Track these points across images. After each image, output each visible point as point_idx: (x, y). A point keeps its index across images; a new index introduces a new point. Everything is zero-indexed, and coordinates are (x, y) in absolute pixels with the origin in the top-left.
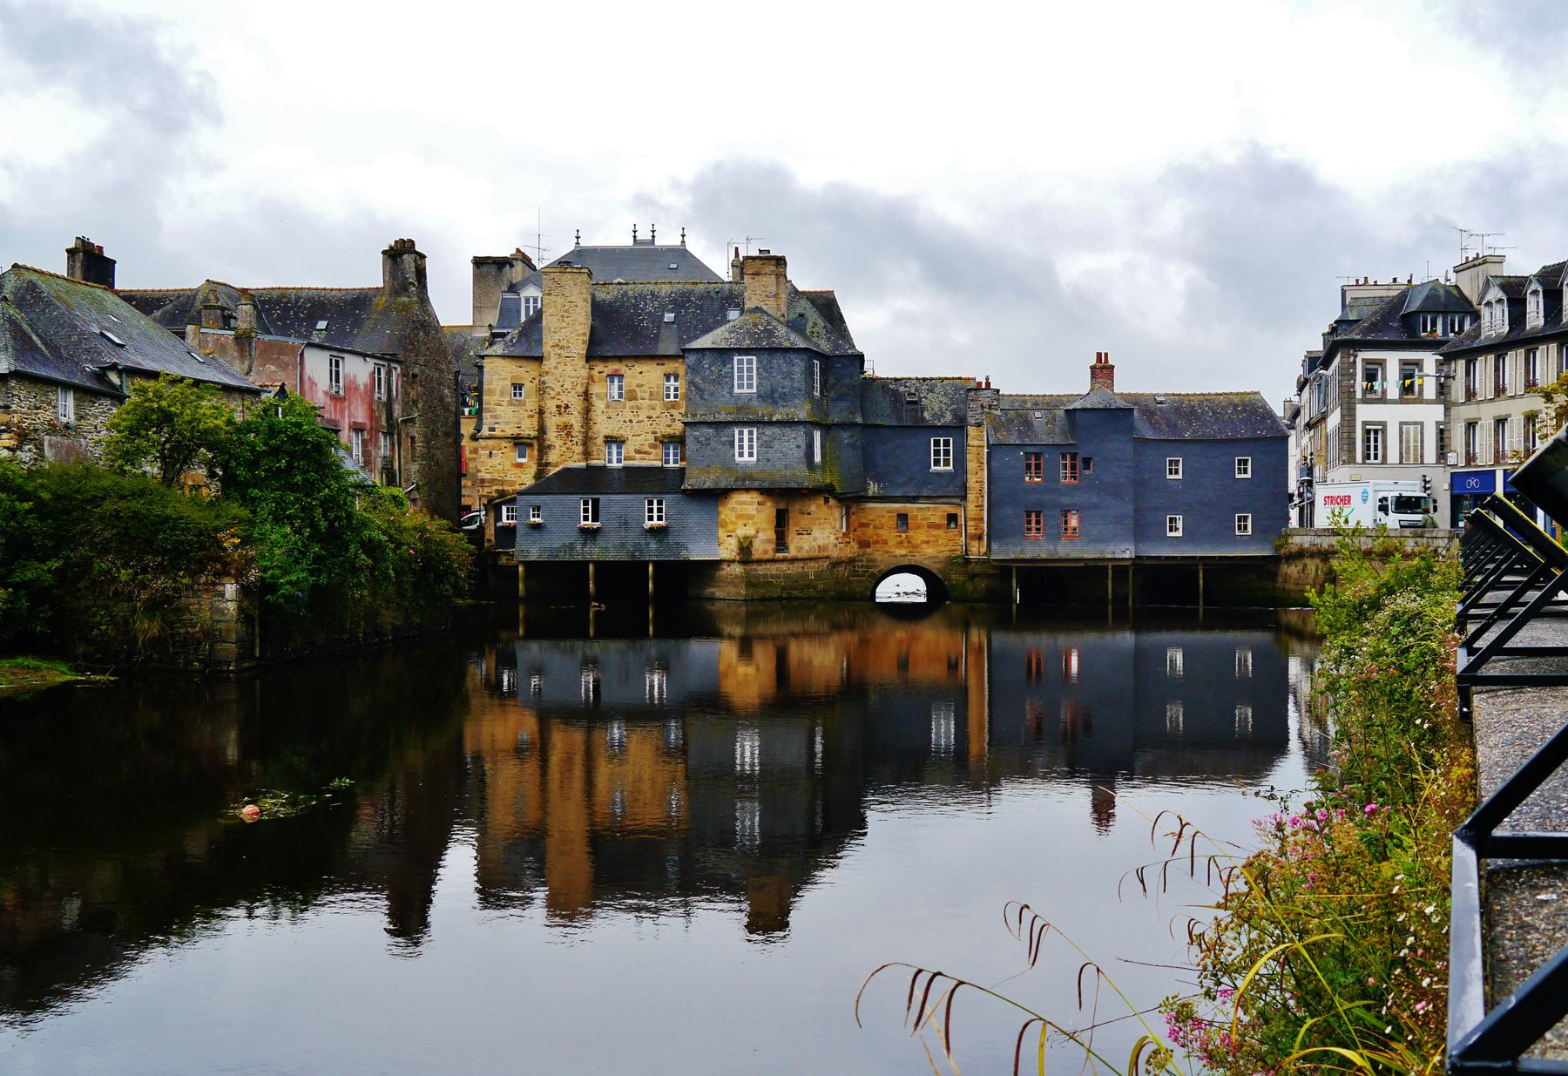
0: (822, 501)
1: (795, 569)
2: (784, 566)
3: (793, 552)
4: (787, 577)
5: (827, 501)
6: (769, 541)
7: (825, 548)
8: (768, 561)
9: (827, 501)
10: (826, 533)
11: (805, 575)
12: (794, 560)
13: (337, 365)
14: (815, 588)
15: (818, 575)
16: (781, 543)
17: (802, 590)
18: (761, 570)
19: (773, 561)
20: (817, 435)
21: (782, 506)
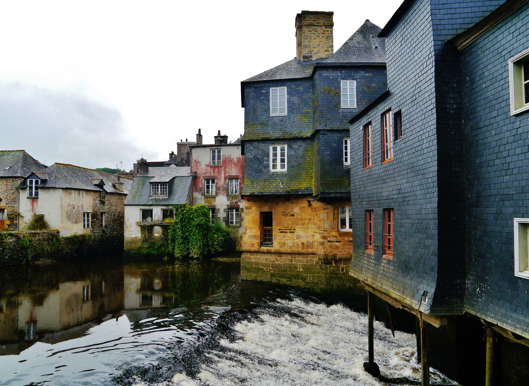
0: (305, 204)
1: (283, 261)
2: (272, 258)
3: (276, 246)
4: (275, 267)
5: (310, 205)
6: (254, 237)
7: (309, 245)
8: (255, 252)
9: (310, 205)
10: (311, 232)
11: (294, 268)
12: (279, 253)
13: (219, 152)
14: (304, 279)
15: (307, 269)
16: (266, 237)
17: (290, 278)
18: (253, 258)
19: (258, 252)
20: (286, 147)
21: (266, 209)
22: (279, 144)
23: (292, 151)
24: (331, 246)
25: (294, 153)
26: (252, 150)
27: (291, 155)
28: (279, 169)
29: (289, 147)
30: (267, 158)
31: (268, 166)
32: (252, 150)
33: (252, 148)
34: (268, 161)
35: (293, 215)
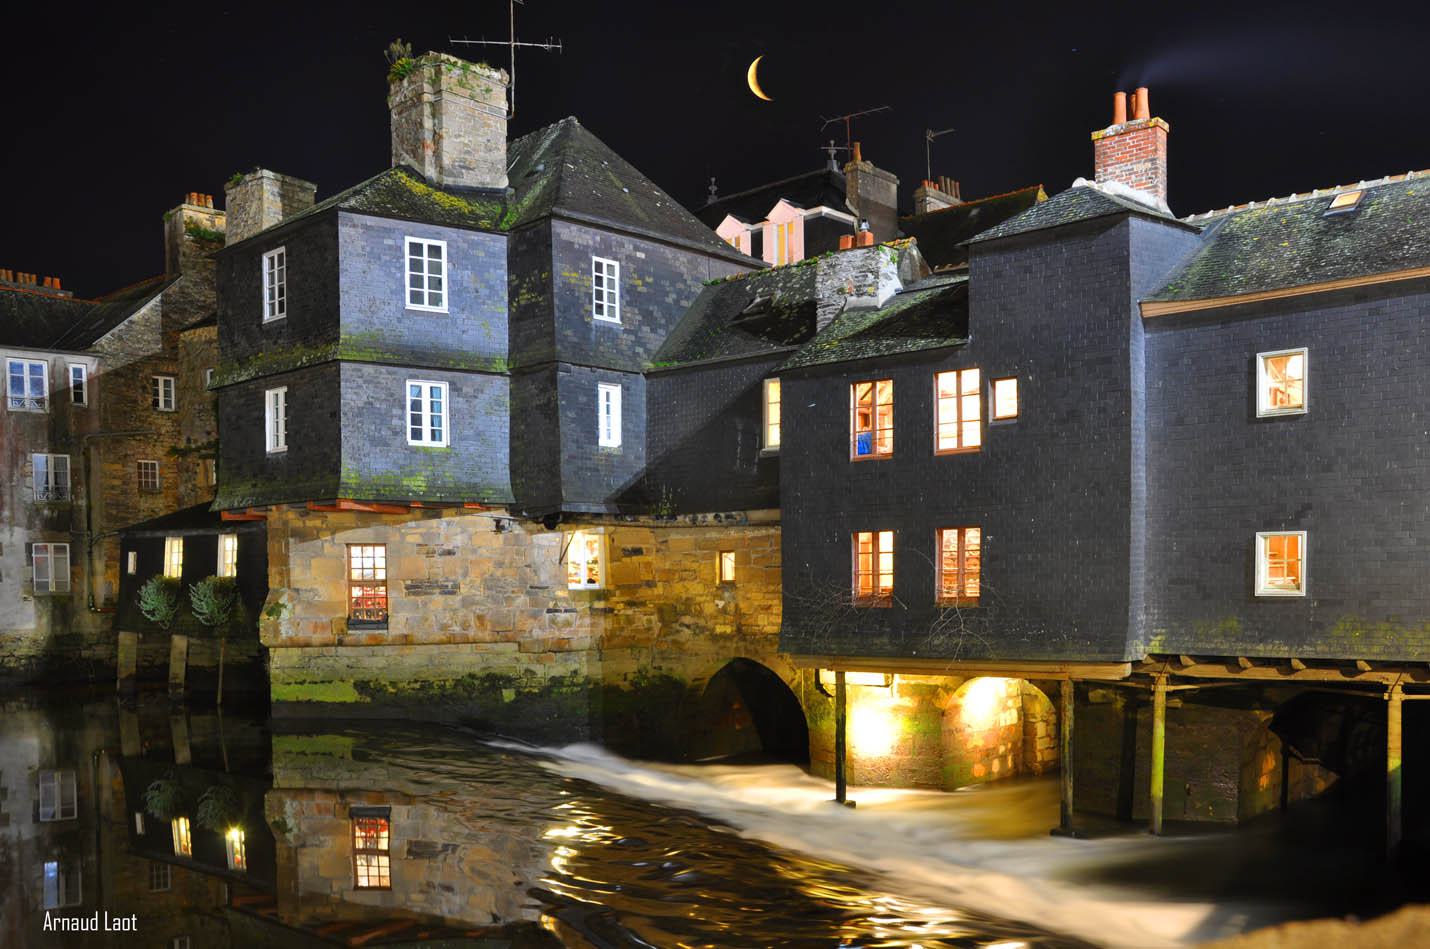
20: (444, 387)
22: (427, 378)
23: (461, 399)
24: (553, 622)
25: (465, 406)
26: (360, 387)
27: (459, 411)
28: (426, 441)
29: (455, 389)
30: (399, 412)
31: (399, 432)
32: (360, 387)
33: (360, 381)
34: (402, 418)
35: (450, 553)
